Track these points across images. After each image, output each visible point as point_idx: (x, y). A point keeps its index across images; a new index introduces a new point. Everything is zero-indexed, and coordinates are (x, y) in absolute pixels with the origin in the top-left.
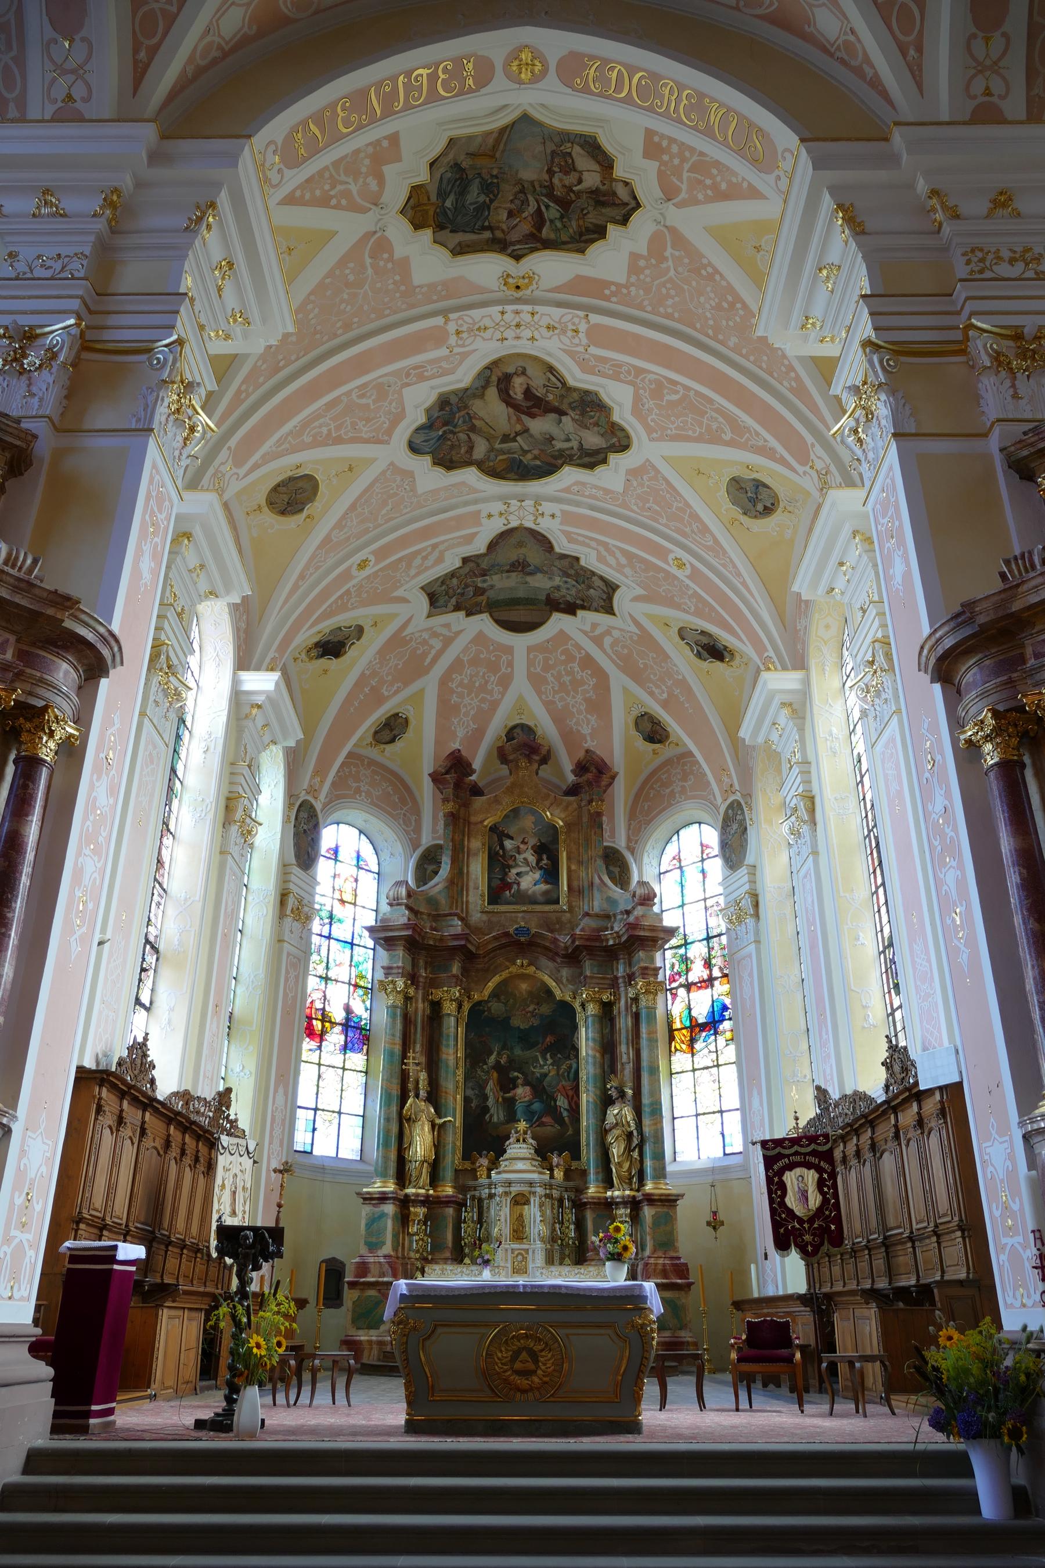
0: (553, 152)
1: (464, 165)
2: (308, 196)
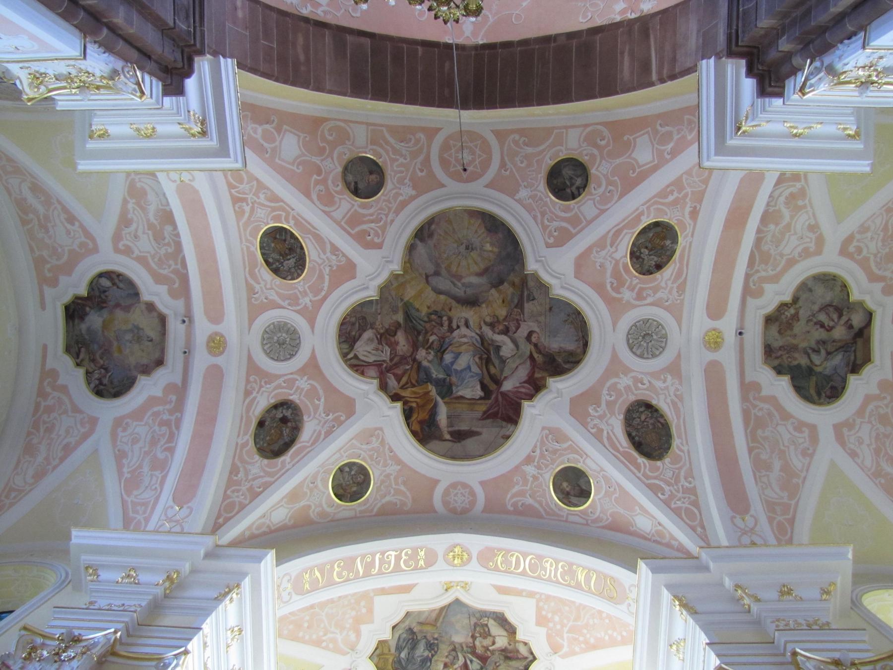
0: (476, 625)
1: (415, 630)
2: (307, 637)
